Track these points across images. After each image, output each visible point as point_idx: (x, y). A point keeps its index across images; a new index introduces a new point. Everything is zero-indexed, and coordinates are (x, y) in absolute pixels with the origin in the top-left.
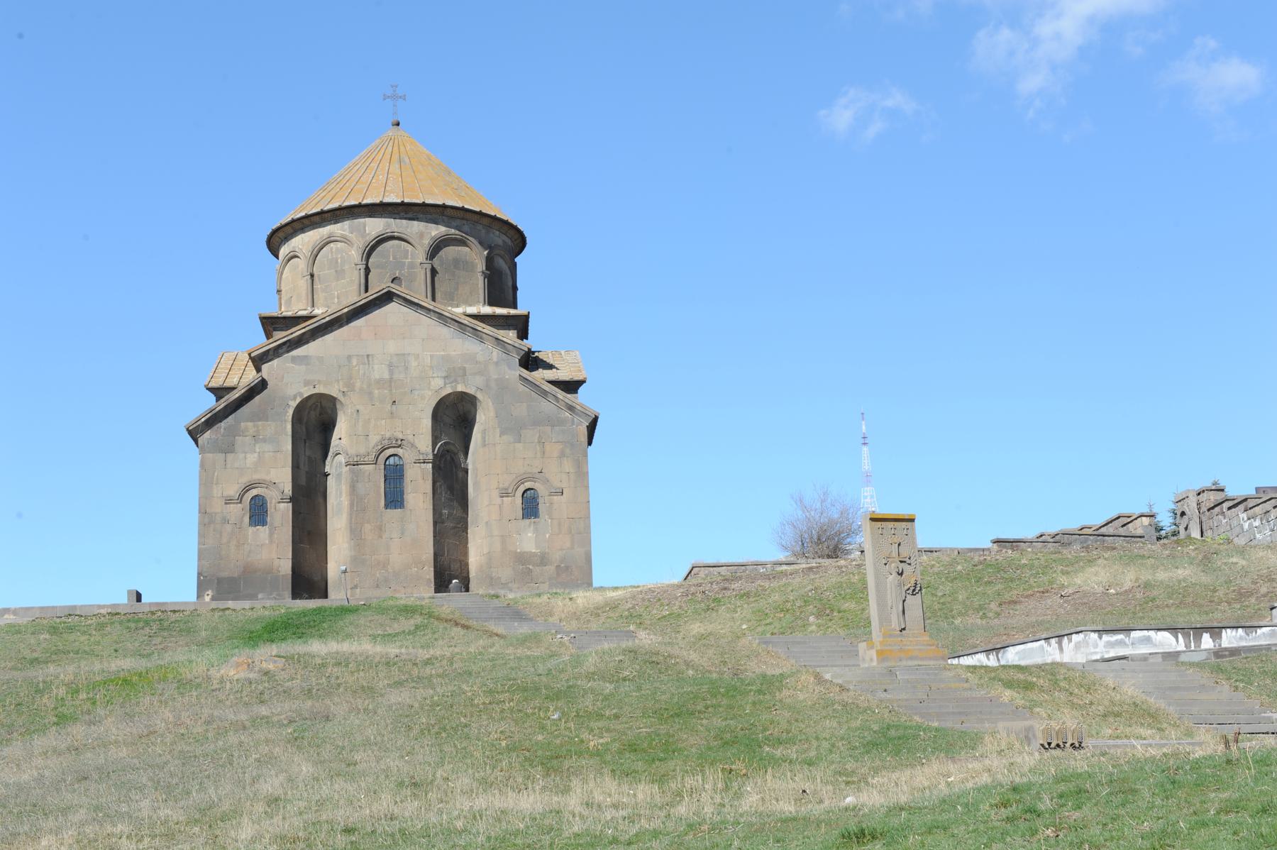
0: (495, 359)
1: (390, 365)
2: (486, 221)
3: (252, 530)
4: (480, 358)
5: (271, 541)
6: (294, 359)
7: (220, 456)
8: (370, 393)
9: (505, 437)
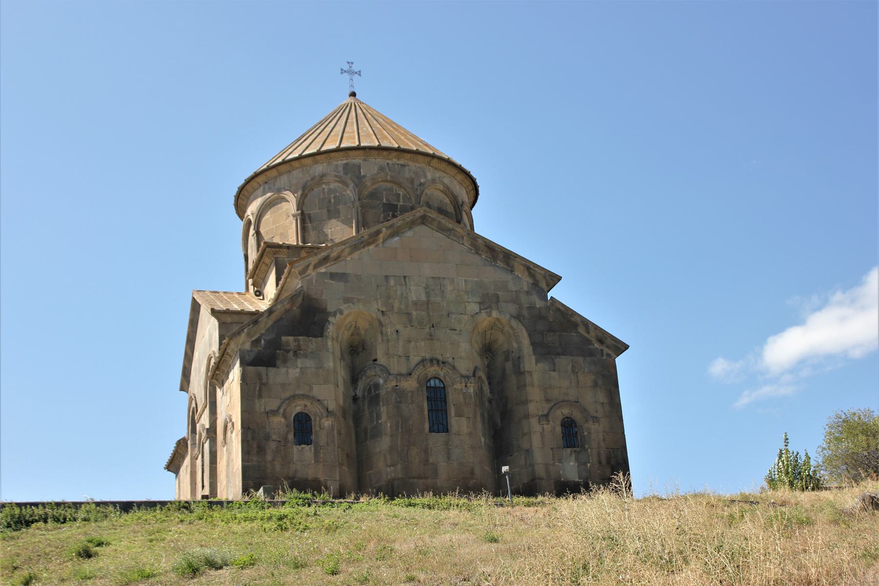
0: (526, 288)
1: (427, 287)
3: (296, 449)
4: (512, 287)
5: (317, 461)
6: (333, 276)
7: (262, 369)
8: (409, 314)
9: (540, 365)
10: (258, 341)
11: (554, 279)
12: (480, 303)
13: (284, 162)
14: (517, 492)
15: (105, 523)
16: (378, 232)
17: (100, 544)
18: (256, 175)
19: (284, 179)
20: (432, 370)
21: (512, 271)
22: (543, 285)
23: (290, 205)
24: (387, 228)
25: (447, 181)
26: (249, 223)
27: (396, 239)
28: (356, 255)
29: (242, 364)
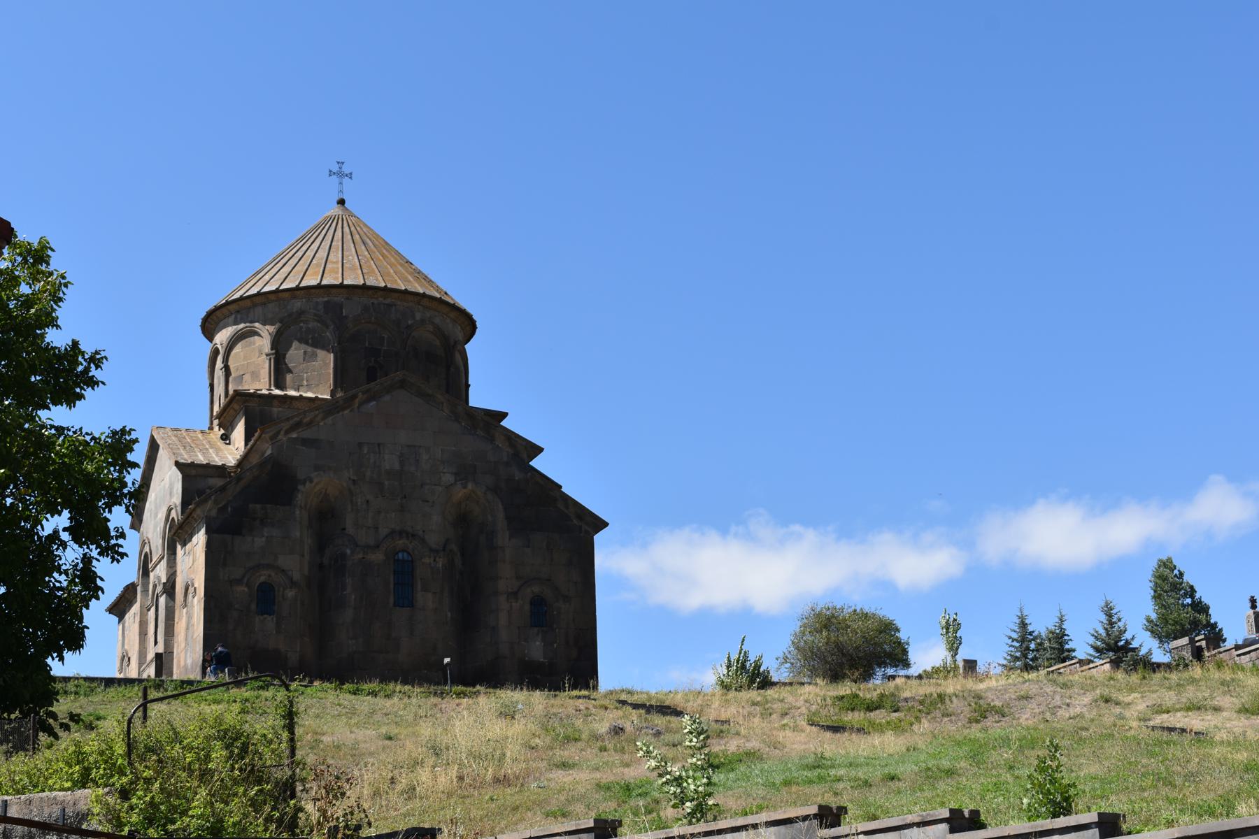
0: (505, 459)
2: (453, 315)
6: (305, 442)
10: (225, 507)
11: (537, 450)
12: (456, 474)
13: (259, 294)
14: (456, 681)
15: (96, 699)
16: (354, 397)
17: (98, 719)
18: (228, 303)
19: (259, 310)
20: (401, 543)
22: (525, 456)
23: (263, 341)
24: (363, 393)
25: (437, 320)
26: (215, 352)
27: (373, 403)
28: (329, 420)
29: (207, 532)
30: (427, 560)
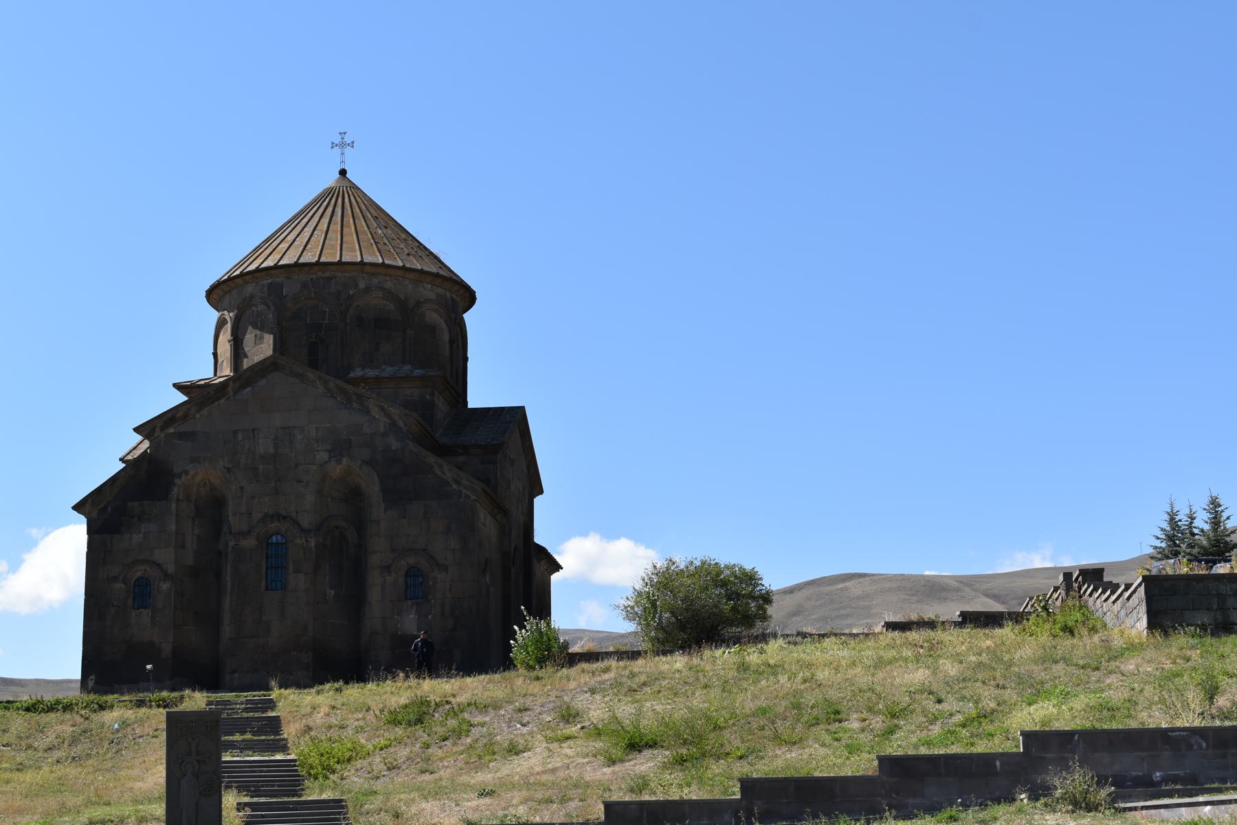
0: (382, 430)
2: (411, 275)
6: (182, 436)
10: (105, 508)
12: (330, 451)
20: (274, 526)
21: (368, 412)
25: (389, 285)
28: (205, 411)
30: (298, 541)
